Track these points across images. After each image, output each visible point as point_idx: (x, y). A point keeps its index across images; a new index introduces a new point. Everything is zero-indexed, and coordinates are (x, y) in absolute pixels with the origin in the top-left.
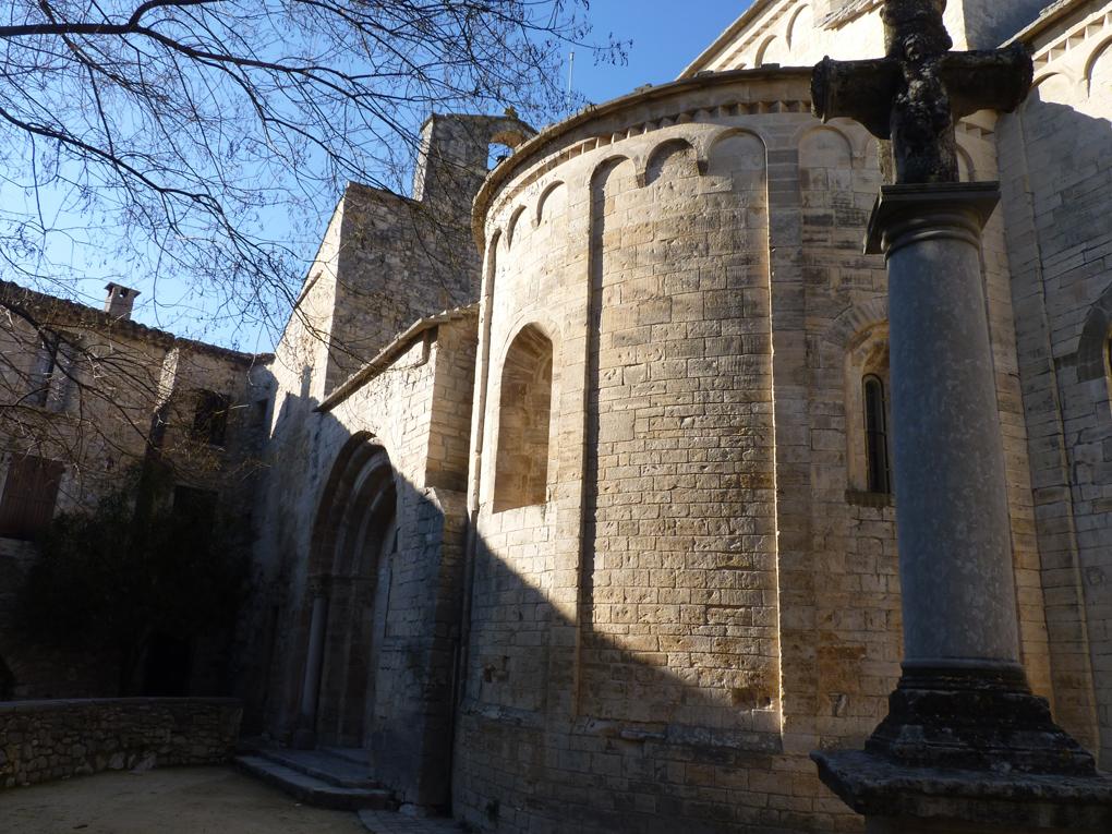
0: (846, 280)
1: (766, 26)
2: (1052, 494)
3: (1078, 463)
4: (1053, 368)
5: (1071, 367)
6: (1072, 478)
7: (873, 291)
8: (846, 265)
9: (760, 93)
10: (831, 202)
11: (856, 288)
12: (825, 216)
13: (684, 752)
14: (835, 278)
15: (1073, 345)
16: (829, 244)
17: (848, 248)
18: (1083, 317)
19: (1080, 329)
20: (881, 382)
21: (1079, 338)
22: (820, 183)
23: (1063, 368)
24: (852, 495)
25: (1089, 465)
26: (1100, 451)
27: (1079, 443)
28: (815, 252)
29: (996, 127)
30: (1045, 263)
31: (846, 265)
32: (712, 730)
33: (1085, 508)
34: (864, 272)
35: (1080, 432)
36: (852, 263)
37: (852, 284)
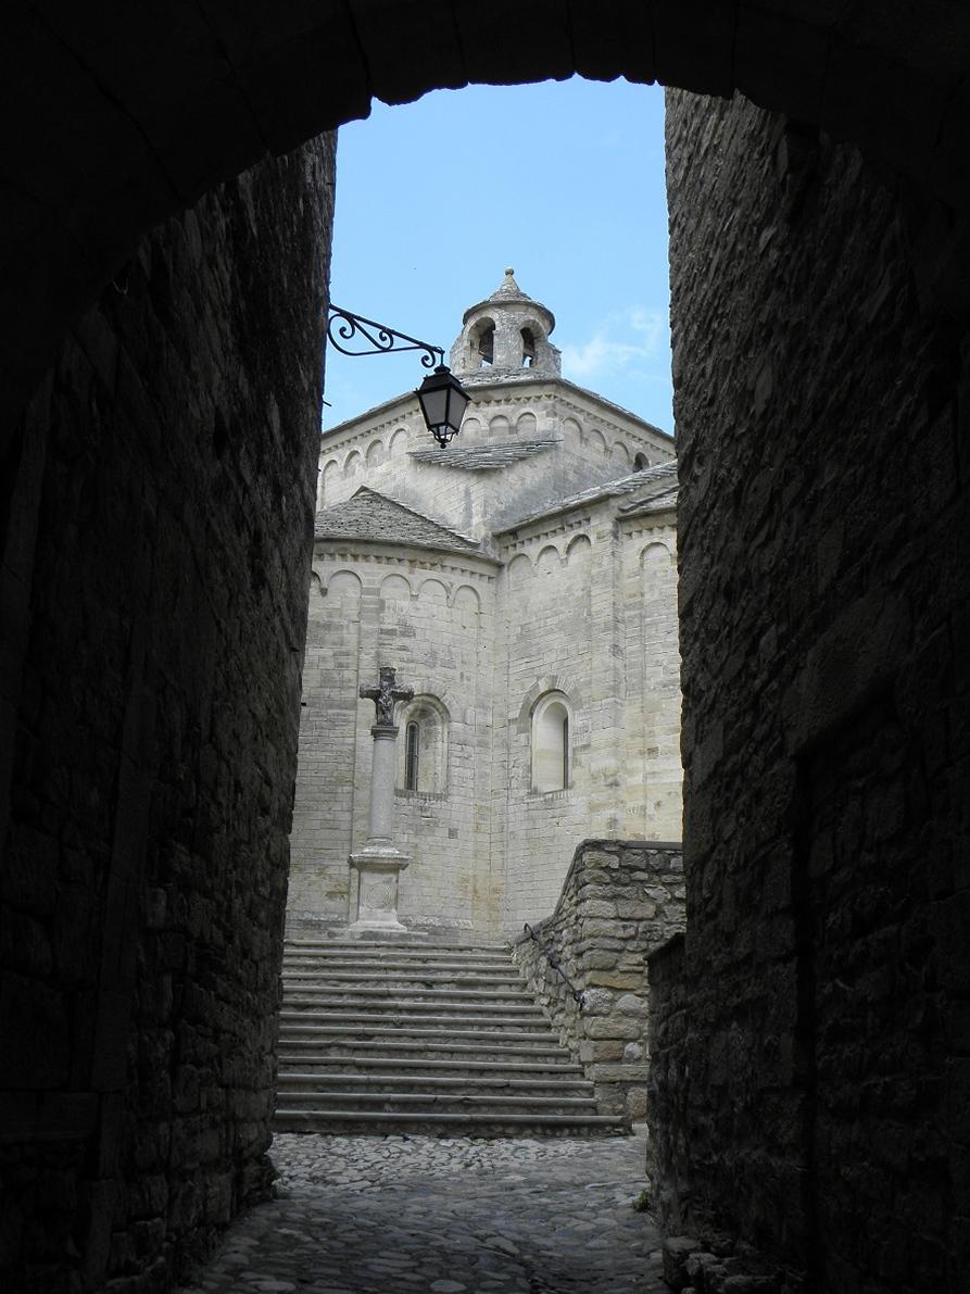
2: (499, 793)
9: (360, 550)
13: (298, 925)
15: (515, 714)
18: (522, 699)
19: (520, 705)
24: (398, 793)
28: (385, 651)
30: (511, 665)
31: (402, 660)
32: (313, 913)
33: (512, 801)
34: (411, 665)
37: (404, 672)
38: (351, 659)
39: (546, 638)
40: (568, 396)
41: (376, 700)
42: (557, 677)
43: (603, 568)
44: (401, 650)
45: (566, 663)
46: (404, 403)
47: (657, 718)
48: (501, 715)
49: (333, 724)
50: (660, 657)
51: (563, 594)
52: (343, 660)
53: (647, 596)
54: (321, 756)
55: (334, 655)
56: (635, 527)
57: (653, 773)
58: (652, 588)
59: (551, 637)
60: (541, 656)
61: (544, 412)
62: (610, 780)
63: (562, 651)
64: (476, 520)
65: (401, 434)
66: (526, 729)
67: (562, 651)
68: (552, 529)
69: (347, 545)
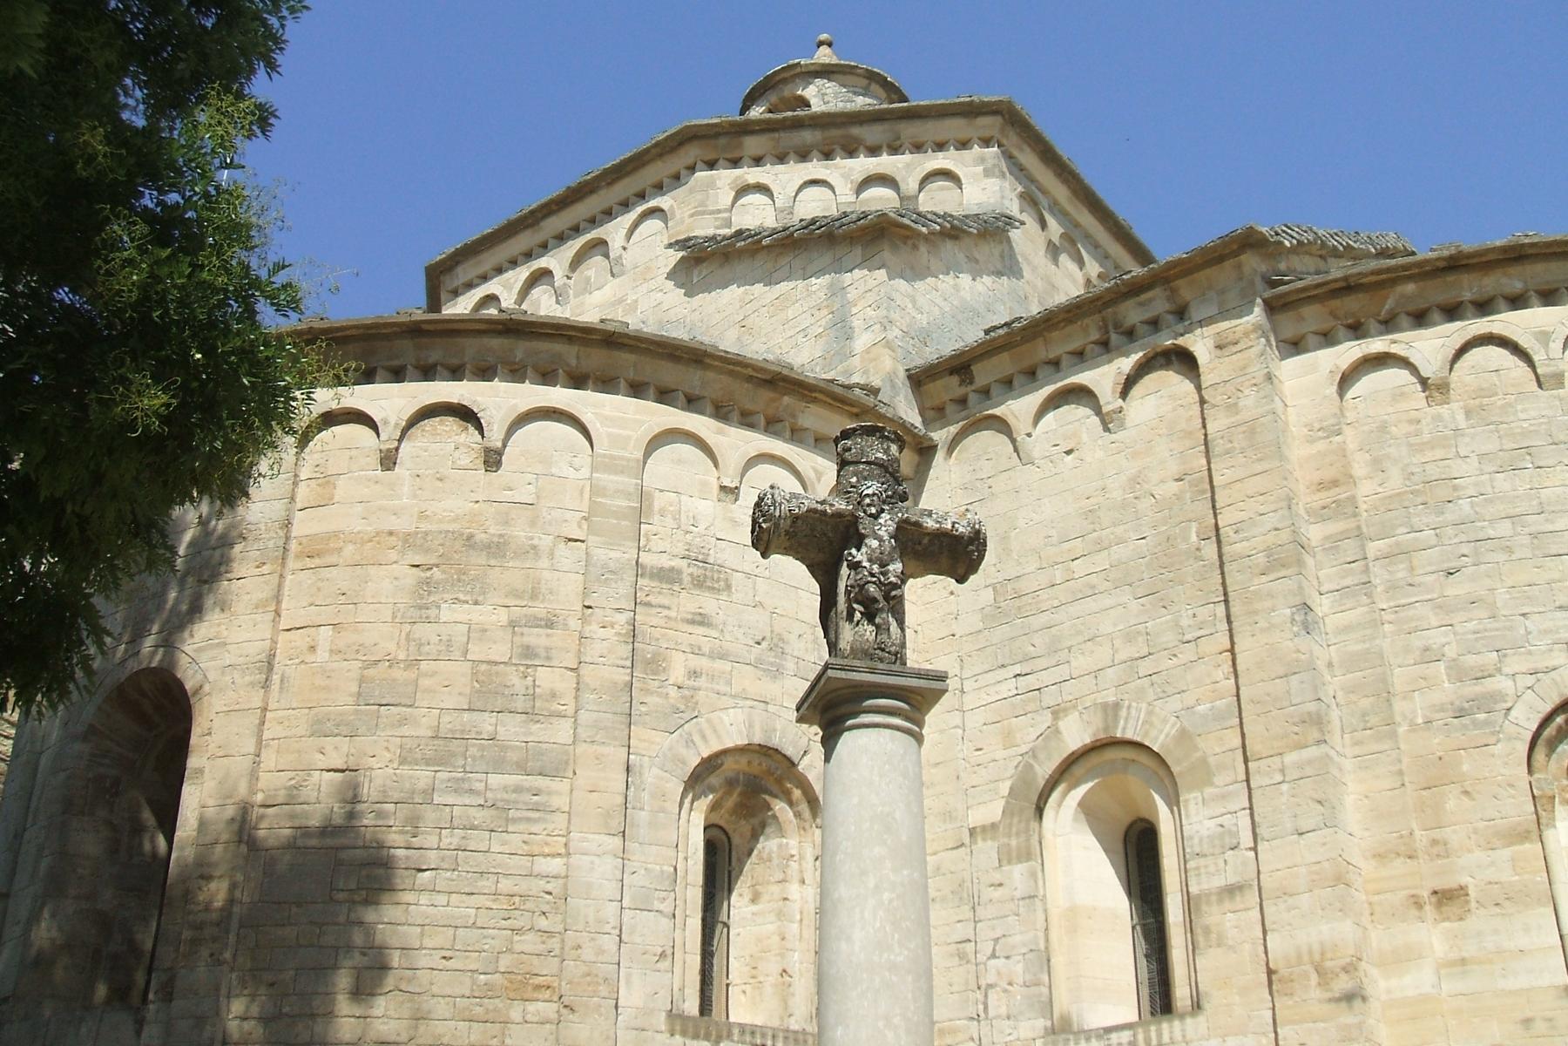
0: (694, 674)
1: (593, 222)
3: (990, 986)
4: (967, 840)
5: (990, 843)
6: (981, 1007)
7: (734, 697)
8: (696, 651)
10: (680, 549)
11: (706, 689)
12: (672, 569)
14: (677, 673)
15: (992, 811)
16: (673, 614)
17: (701, 624)
18: (1011, 771)
19: (1005, 788)
20: (729, 838)
21: (1002, 802)
22: (669, 521)
23: (980, 842)
25: (1005, 991)
26: (1019, 968)
27: (993, 956)
29: (916, 472)
35: (996, 940)
36: (706, 650)
37: (702, 682)
38: (556, 638)
39: (1074, 609)
40: (1021, 150)
41: (826, 576)
42: (1117, 706)
43: (1245, 415)
44: (692, 622)
45: (1145, 667)
46: (660, 155)
47: (1451, 804)
48: (948, 816)
49: (502, 813)
50: (1436, 638)
51: (1117, 495)
52: (537, 637)
53: (1366, 490)
54: (463, 909)
55: (513, 624)
56: (1313, 317)
57: (1463, 962)
58: (1378, 465)
59: (1090, 605)
60: (1063, 655)
61: (980, 169)
62: (1343, 984)
63: (1129, 638)
64: (862, 342)
65: (653, 224)
66: (1030, 853)
67: (1129, 638)
68: (1075, 345)
69: (558, 347)
